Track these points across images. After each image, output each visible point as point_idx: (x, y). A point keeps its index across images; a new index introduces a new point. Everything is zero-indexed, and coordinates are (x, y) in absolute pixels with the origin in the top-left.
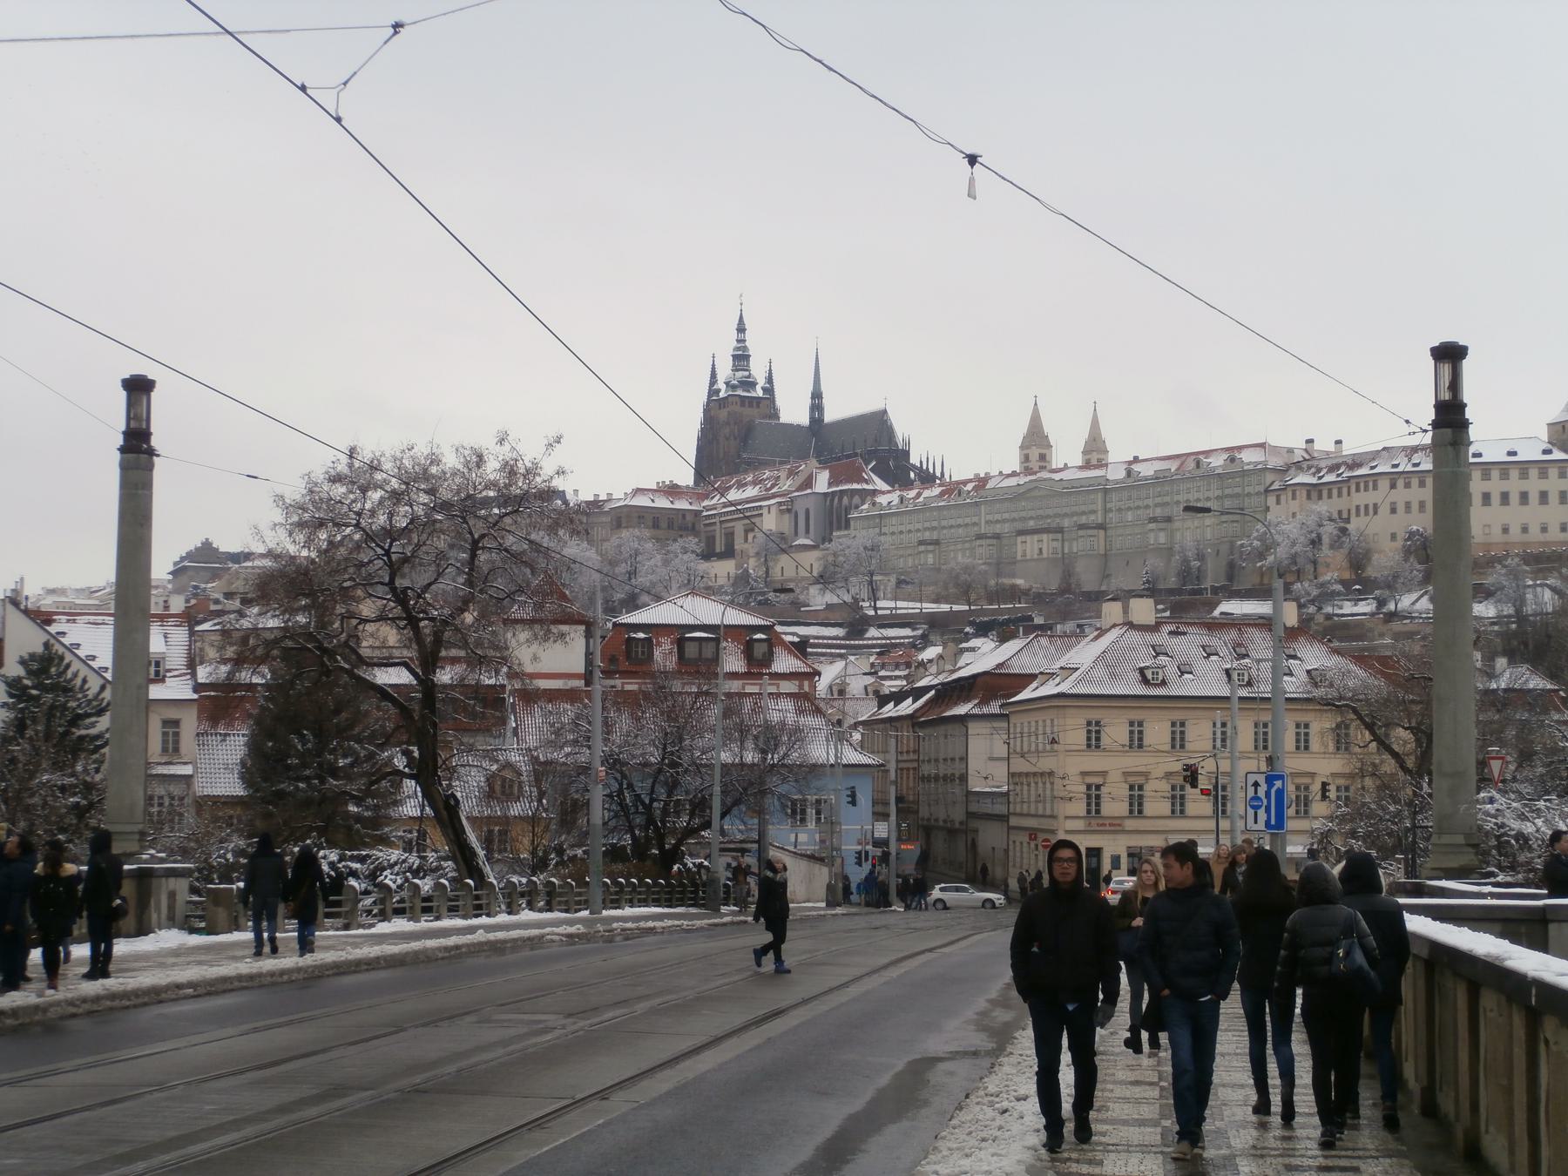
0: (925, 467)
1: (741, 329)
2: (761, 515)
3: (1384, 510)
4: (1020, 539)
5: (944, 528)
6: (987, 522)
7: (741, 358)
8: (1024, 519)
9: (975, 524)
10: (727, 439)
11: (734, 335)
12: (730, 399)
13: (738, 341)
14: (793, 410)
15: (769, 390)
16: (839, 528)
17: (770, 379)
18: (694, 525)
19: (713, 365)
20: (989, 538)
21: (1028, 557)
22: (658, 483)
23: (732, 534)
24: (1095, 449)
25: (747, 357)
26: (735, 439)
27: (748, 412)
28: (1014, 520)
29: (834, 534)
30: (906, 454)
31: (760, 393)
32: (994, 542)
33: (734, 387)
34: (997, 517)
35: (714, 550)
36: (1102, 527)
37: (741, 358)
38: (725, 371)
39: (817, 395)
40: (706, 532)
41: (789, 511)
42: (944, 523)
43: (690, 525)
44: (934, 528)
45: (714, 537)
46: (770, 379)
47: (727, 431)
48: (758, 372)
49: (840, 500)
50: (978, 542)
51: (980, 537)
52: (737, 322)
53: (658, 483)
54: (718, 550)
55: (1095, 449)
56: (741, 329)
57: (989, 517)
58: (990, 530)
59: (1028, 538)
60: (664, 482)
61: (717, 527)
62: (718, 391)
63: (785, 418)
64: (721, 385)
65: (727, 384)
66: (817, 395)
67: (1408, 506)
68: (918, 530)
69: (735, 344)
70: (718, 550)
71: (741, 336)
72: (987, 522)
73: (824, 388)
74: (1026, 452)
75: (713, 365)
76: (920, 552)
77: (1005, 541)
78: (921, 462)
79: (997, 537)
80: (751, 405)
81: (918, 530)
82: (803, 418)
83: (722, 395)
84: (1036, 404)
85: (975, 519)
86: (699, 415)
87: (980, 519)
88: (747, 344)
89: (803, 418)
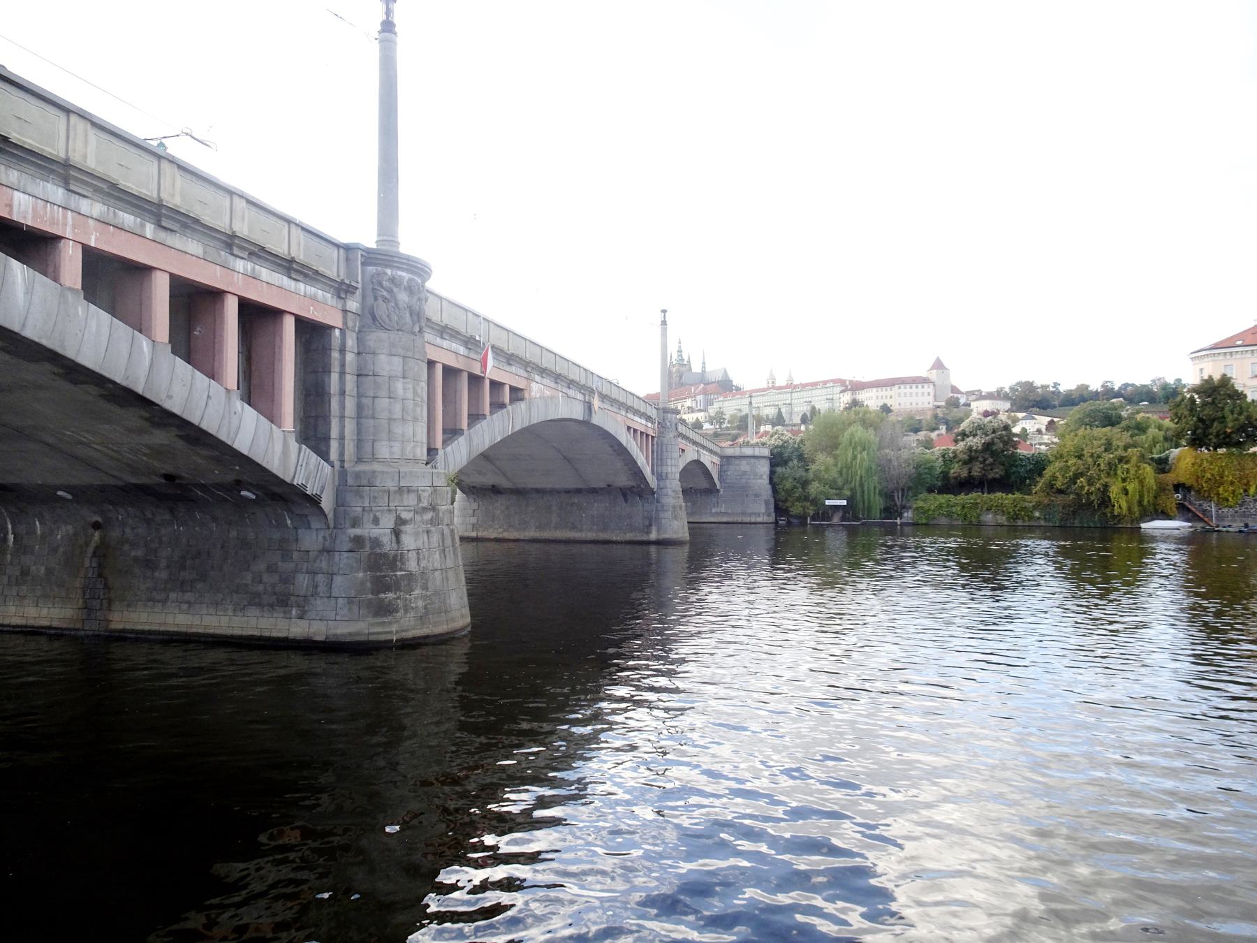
3: (874, 398)
7: (680, 351)
14: (696, 368)
15: (689, 362)
24: (791, 378)
27: (683, 369)
31: (685, 362)
36: (790, 404)
37: (680, 351)
39: (704, 363)
48: (685, 357)
55: (791, 378)
63: (693, 371)
64: (673, 360)
66: (704, 363)
67: (882, 397)
79: (758, 407)
82: (700, 371)
89: (700, 371)
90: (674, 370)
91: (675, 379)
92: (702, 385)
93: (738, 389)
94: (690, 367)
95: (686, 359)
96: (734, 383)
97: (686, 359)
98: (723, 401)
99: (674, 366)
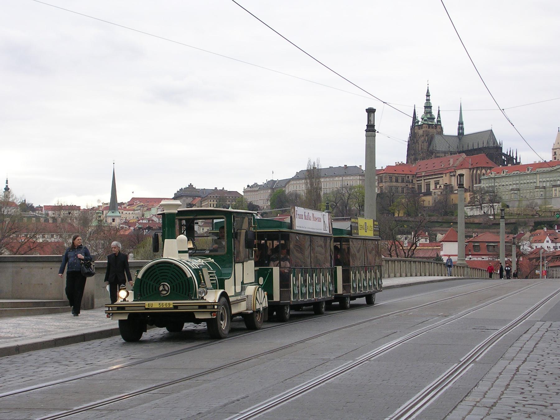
0: (508, 154)
1: (428, 95)
2: (442, 177)
4: (554, 189)
5: (521, 184)
6: (540, 182)
7: (428, 107)
8: (555, 181)
9: (535, 182)
10: (423, 143)
11: (425, 98)
12: (424, 125)
13: (427, 100)
15: (439, 121)
16: (476, 183)
17: (439, 114)
18: (412, 180)
19: (415, 109)
20: (541, 188)
21: (557, 196)
22: (396, 163)
23: (429, 184)
25: (430, 107)
26: (426, 142)
28: (551, 181)
29: (474, 185)
30: (501, 148)
32: (543, 190)
33: (425, 120)
34: (544, 180)
35: (421, 191)
37: (428, 107)
38: (420, 114)
39: (461, 123)
40: (418, 184)
41: (454, 175)
42: (522, 182)
43: (411, 181)
44: (517, 184)
45: (421, 186)
46: (439, 114)
47: (422, 139)
48: (435, 113)
49: (477, 172)
50: (536, 190)
51: (537, 187)
52: (426, 92)
53: (396, 163)
54: (423, 191)
56: (428, 95)
57: (541, 180)
58: (541, 185)
59: (557, 188)
60: (398, 162)
61: (423, 182)
62: (418, 122)
63: (446, 132)
64: (419, 118)
65: (422, 119)
66: (461, 123)
68: (510, 185)
69: (426, 101)
70: (423, 191)
71: (428, 98)
72: (540, 182)
73: (463, 120)
74: (555, 151)
75: (415, 109)
76: (512, 194)
77: (547, 189)
78: (507, 152)
79: (544, 188)
80: (432, 128)
81: (510, 185)
83: (420, 123)
84: (559, 131)
85: (535, 180)
86: (409, 131)
87: (537, 180)
88: (430, 101)
89: (457, 135)
90: (421, 132)
91: (422, 145)
92: (464, 155)
93: (510, 159)
94: (442, 128)
95: (436, 116)
96: (504, 151)
97: (436, 116)
98: (494, 178)
99: (420, 127)
